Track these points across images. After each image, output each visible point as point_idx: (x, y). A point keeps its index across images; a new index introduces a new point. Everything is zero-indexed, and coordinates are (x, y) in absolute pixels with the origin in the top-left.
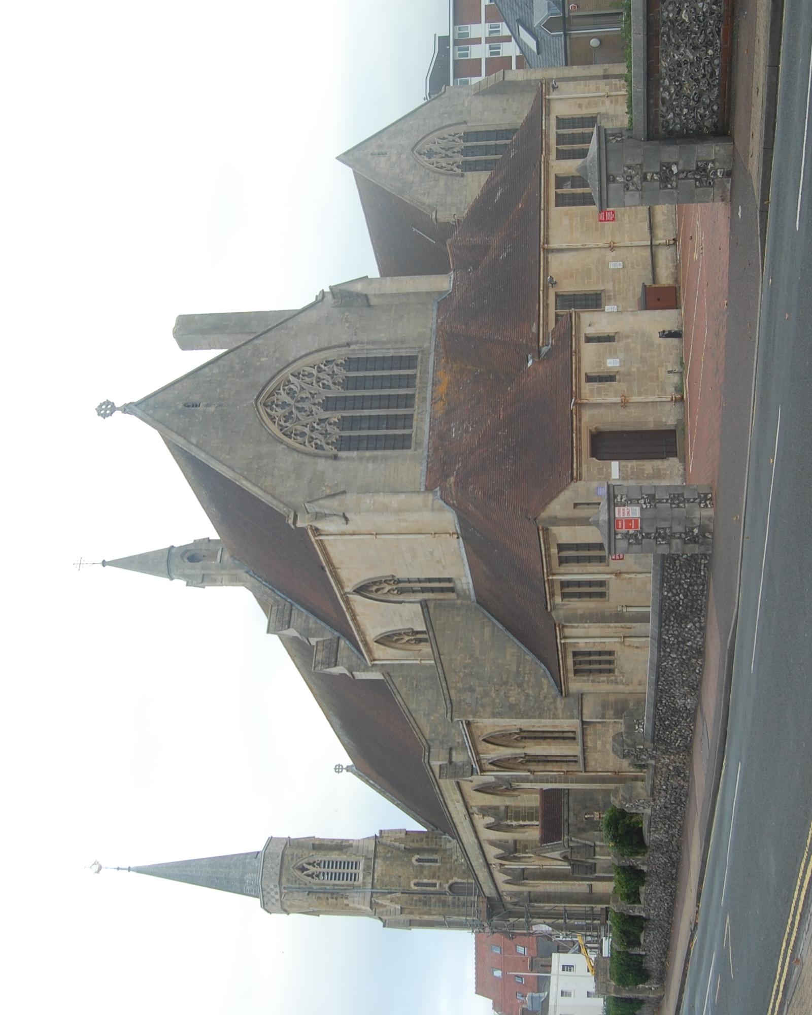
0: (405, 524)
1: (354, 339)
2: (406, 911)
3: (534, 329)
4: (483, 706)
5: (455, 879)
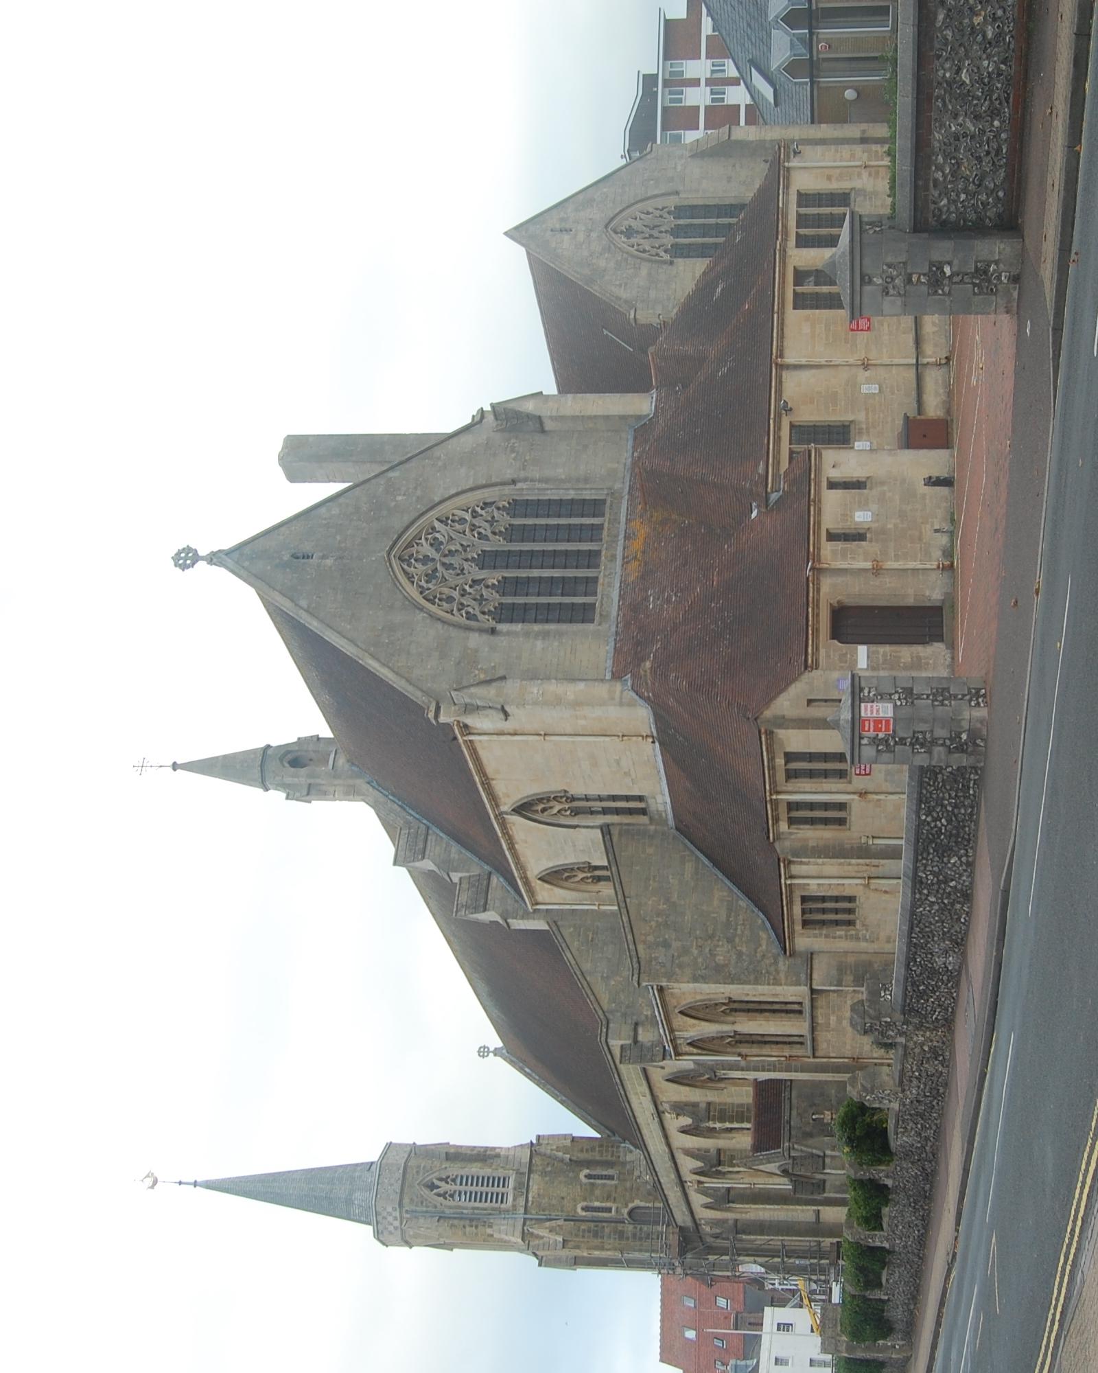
0: (583, 722)
1: (522, 474)
2: (571, 1244)
3: (761, 469)
4: (680, 966)
5: (637, 1203)
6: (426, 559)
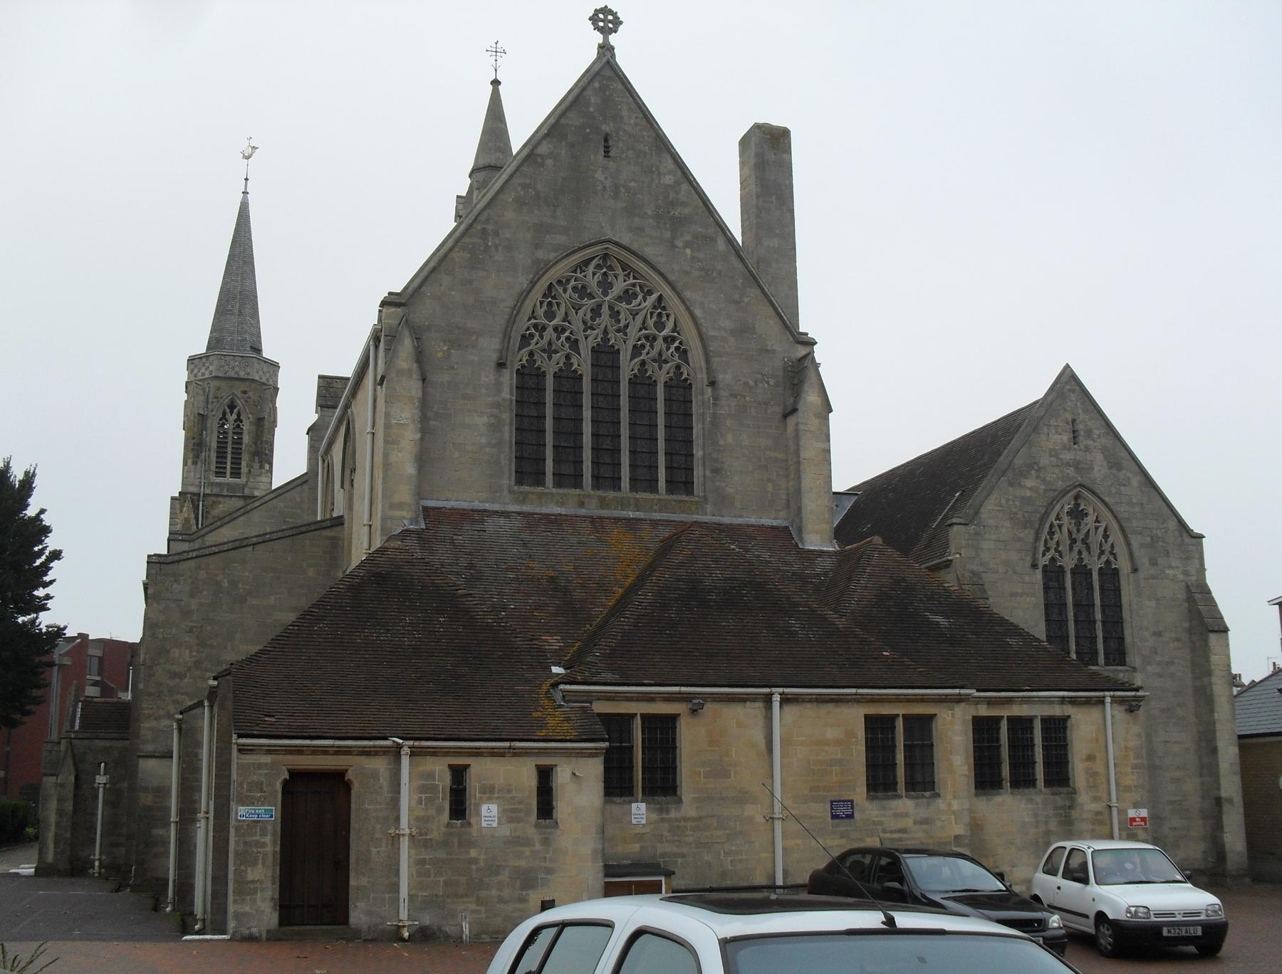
1: (724, 393)
6: (606, 286)
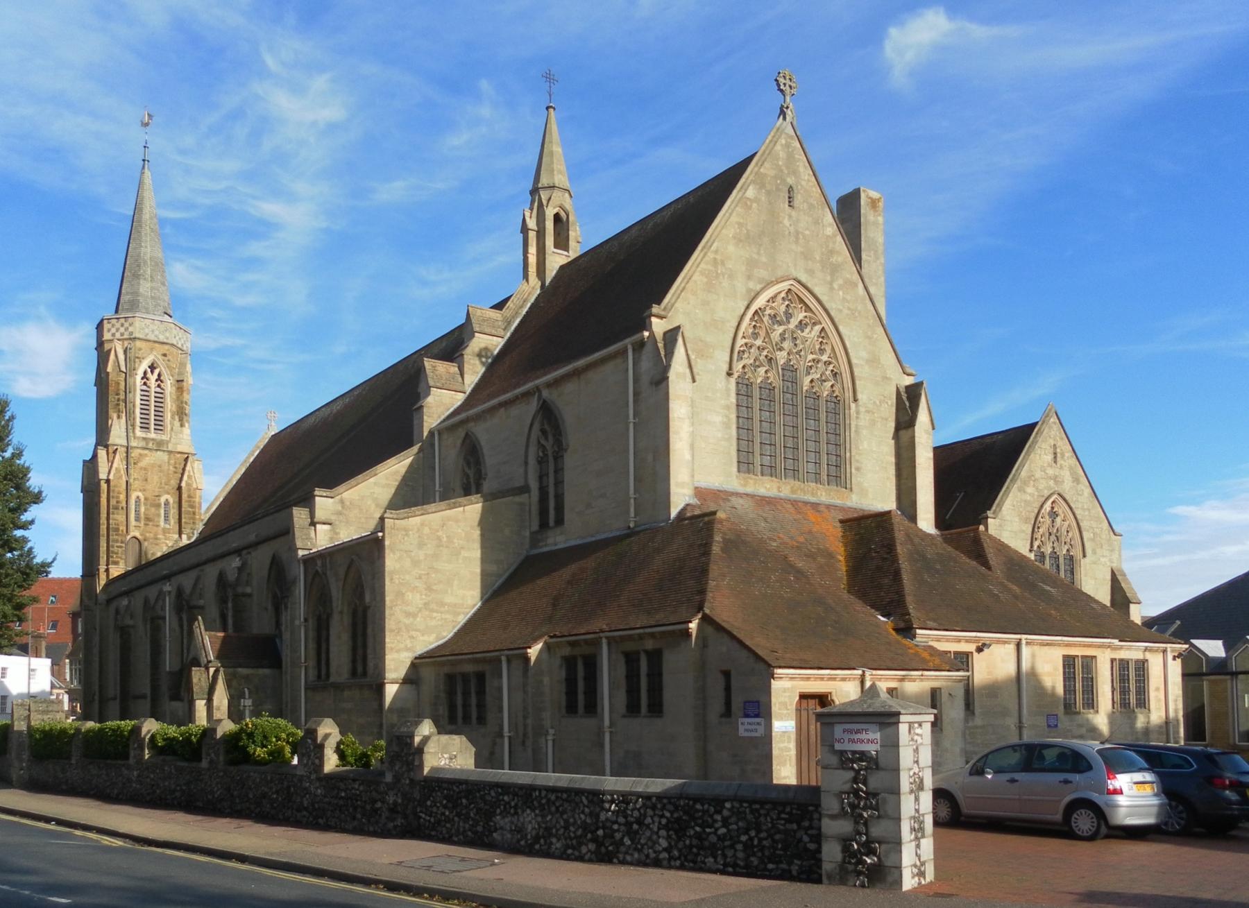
0: (650, 458)
1: (862, 409)
6: (789, 316)
